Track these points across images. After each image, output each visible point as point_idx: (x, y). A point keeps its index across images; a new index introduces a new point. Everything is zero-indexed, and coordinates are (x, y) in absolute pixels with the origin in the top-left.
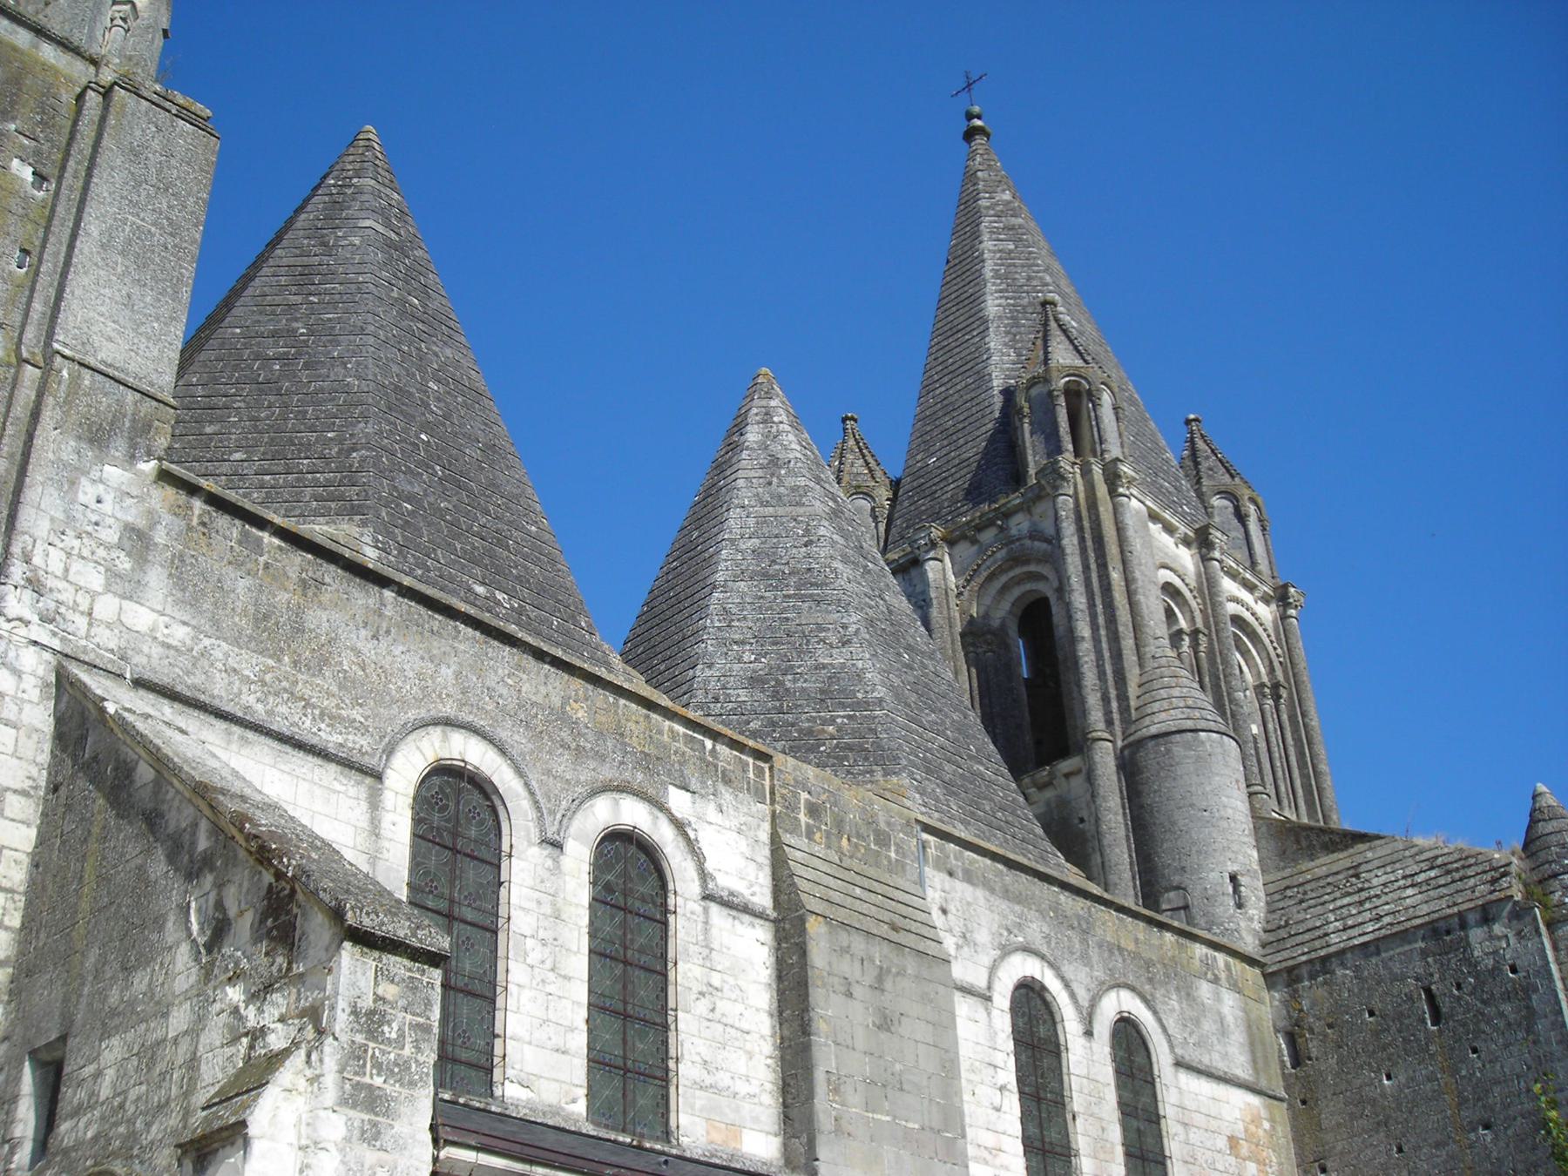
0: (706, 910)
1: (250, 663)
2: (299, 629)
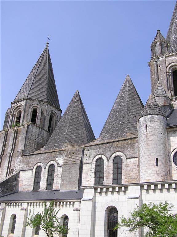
1: (26, 166)
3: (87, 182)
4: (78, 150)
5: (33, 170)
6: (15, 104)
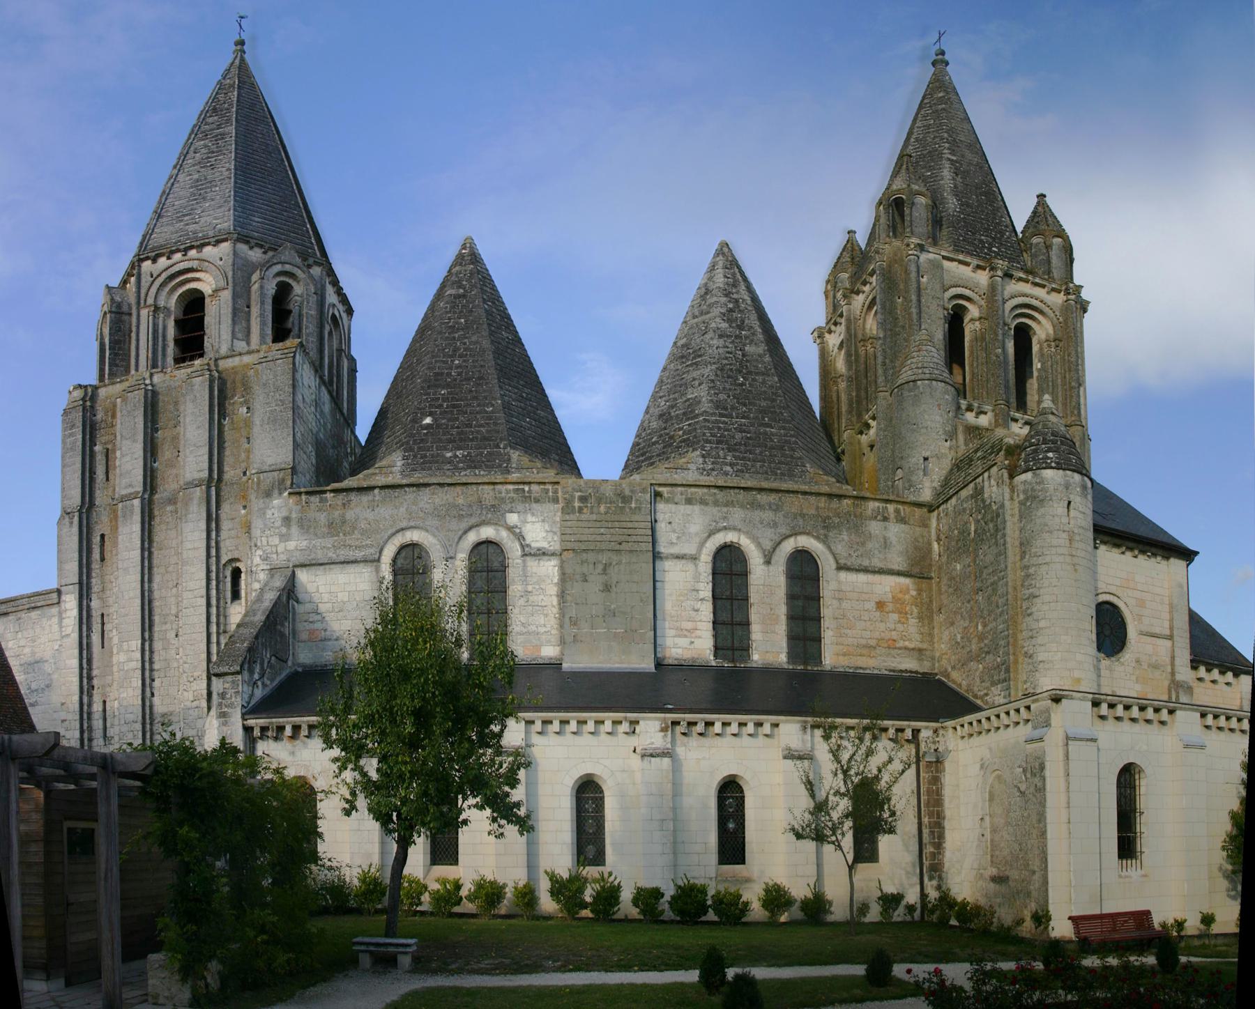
0: (524, 561)
1: (328, 542)
2: (344, 522)
3: (679, 636)
4: (627, 492)
5: (378, 560)
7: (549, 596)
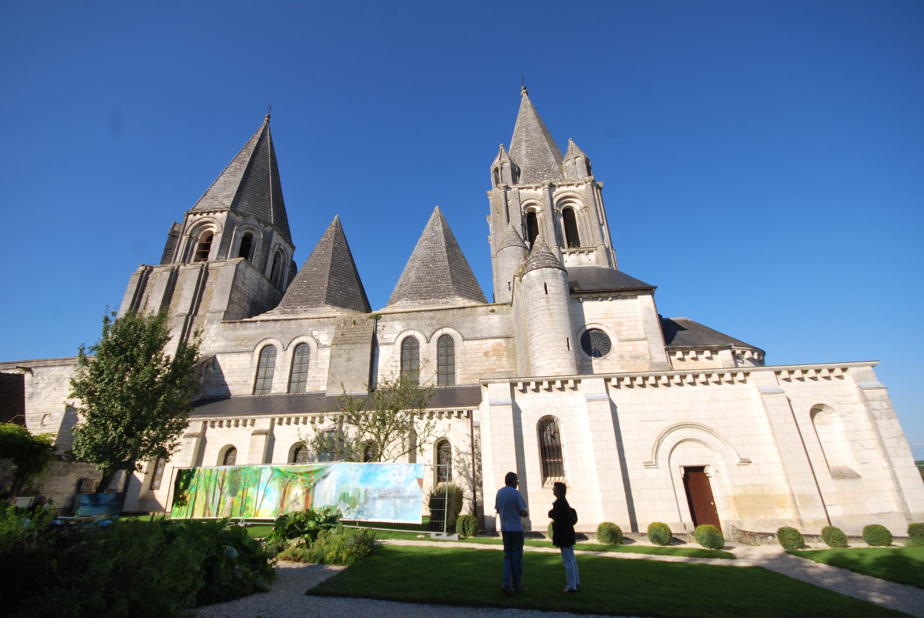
6: (198, 216)
7: (326, 365)
